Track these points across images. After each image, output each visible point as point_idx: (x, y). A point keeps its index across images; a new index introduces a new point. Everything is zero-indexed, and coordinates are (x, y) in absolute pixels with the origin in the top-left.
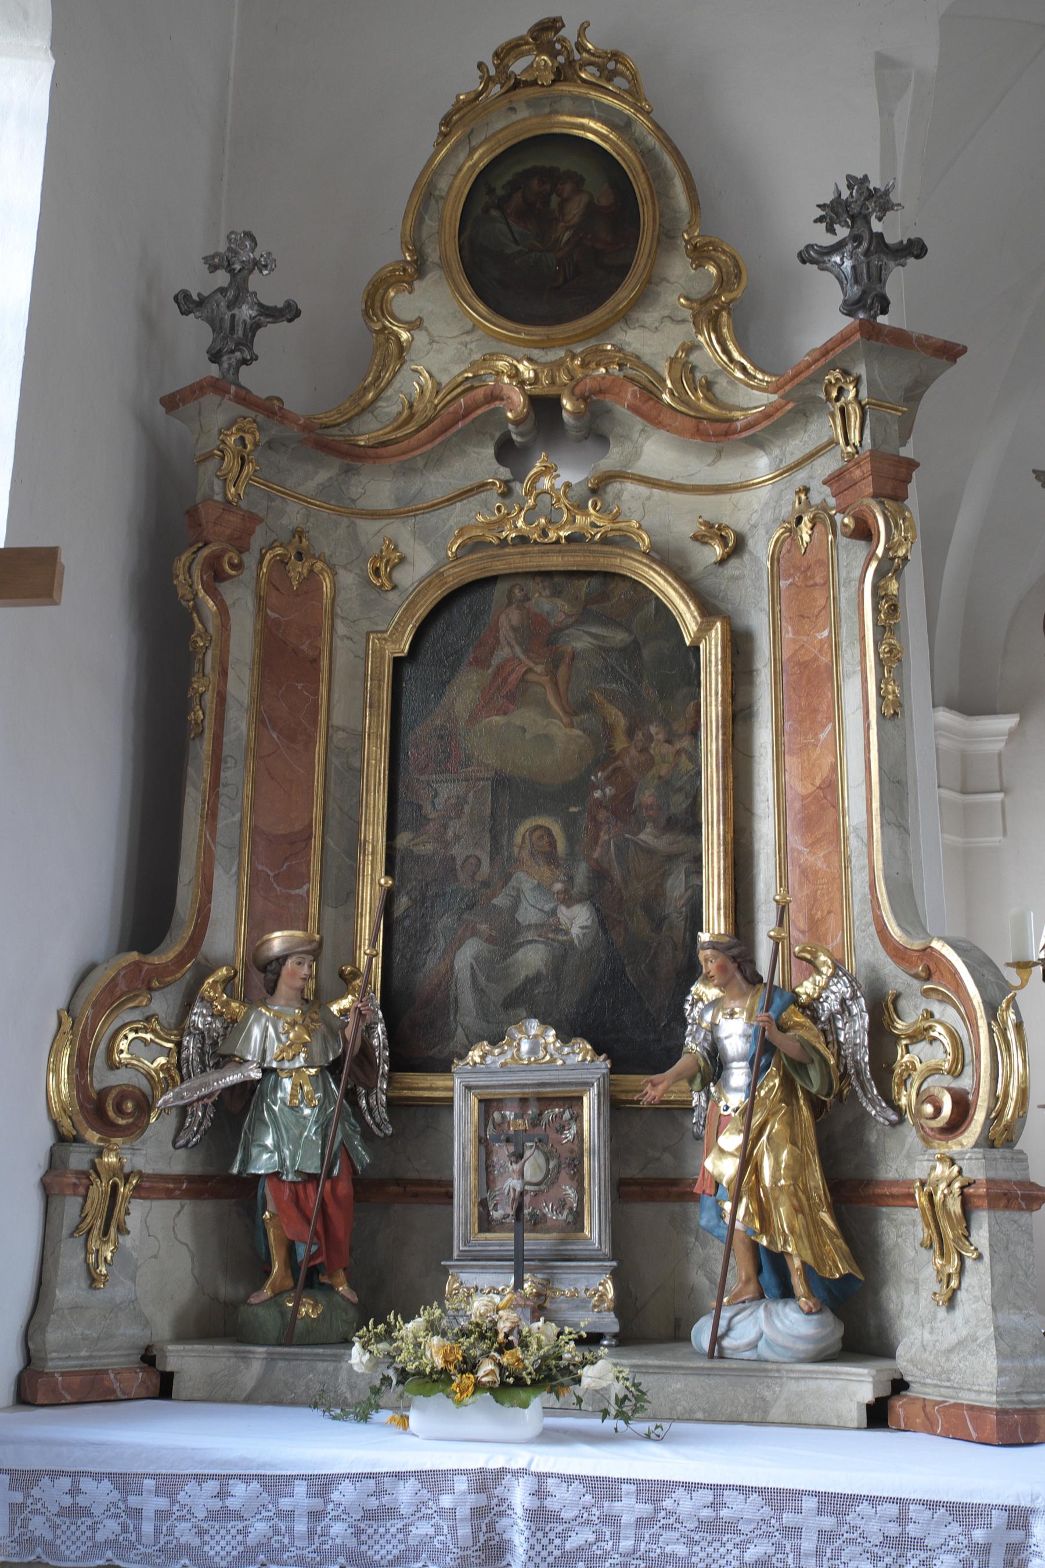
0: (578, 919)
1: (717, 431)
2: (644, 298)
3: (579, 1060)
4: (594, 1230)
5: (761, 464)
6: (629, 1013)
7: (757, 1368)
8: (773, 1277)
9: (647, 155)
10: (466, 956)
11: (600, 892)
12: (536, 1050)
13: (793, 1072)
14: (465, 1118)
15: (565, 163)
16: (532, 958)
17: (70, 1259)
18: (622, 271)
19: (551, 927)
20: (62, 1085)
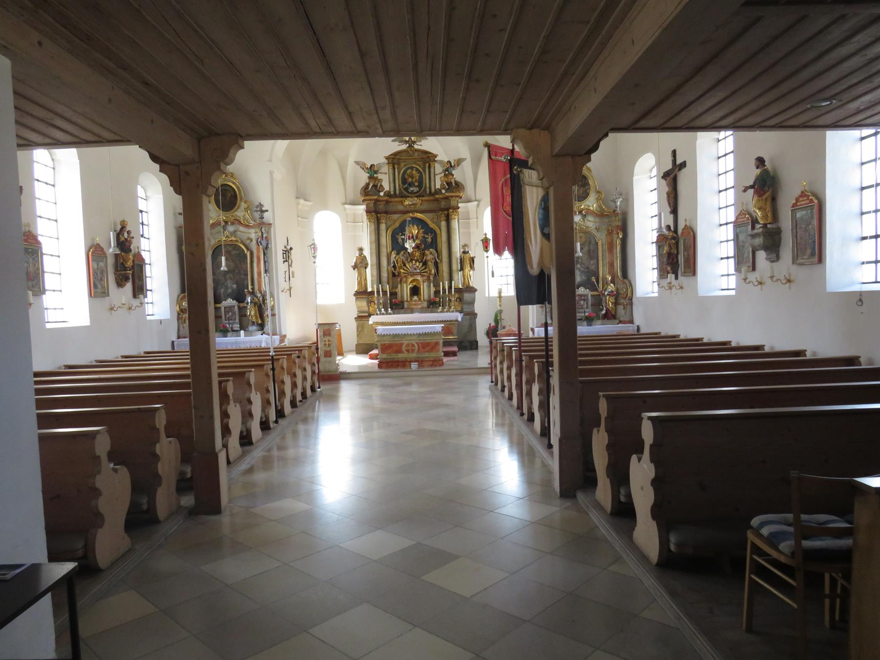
0: (235, 286)
1: (248, 226)
2: (238, 207)
3: (234, 303)
4: (237, 320)
5: (253, 231)
6: (240, 298)
7: (252, 332)
8: (253, 323)
9: (238, 188)
10: (222, 290)
11: (237, 283)
12: (230, 302)
13: (255, 304)
14: (223, 309)
15: (227, 188)
16: (230, 291)
17: (181, 326)
18: (235, 204)
19: (232, 287)
20: (178, 308)
